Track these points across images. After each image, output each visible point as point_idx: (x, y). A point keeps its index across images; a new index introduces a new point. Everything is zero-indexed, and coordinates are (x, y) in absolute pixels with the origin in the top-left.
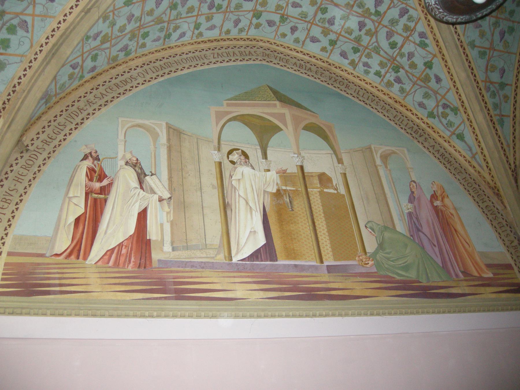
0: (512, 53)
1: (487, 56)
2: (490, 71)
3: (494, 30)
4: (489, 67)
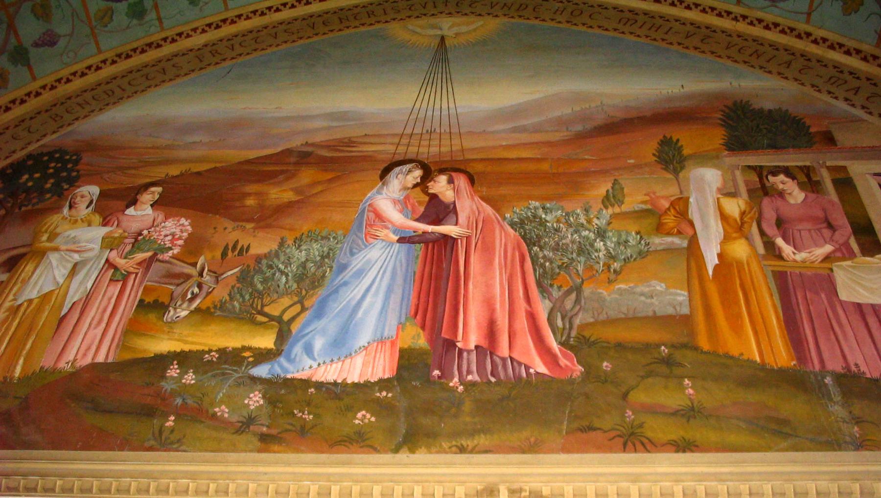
0: (97, 44)
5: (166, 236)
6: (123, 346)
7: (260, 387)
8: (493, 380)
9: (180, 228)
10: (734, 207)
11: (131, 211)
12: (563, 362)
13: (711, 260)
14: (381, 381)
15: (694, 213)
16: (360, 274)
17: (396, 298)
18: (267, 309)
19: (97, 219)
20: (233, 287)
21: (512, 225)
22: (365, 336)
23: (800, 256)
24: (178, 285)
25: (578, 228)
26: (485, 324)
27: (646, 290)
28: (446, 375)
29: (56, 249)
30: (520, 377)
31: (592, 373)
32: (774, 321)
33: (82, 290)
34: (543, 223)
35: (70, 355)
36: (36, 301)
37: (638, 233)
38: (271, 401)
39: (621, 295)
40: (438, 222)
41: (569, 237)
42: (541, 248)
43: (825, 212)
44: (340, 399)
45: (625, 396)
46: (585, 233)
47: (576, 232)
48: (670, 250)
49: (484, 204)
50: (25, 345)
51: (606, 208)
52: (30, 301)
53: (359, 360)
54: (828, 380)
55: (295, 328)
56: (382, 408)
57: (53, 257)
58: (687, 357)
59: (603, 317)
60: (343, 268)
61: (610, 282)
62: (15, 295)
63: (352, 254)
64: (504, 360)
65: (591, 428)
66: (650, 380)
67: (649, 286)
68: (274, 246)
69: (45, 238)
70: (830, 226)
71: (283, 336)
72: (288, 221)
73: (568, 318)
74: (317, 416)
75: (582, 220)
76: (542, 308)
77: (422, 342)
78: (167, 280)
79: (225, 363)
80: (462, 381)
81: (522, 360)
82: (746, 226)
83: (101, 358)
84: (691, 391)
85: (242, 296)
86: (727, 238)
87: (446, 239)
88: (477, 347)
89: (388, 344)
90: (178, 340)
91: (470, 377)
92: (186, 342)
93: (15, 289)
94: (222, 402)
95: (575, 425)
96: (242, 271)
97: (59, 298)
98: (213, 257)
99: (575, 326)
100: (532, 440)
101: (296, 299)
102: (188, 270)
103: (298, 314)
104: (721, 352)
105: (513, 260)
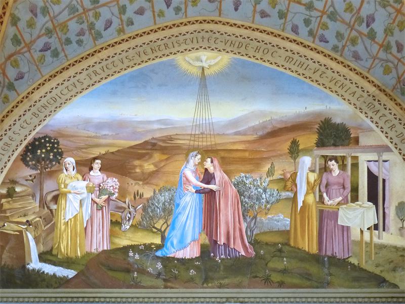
1: (18, 48)
2: (11, 63)
3: (43, 35)
4: (12, 59)
5: (110, 187)
6: (111, 242)
7: (160, 260)
8: (229, 258)
9: (114, 183)
10: (313, 177)
11: (91, 173)
12: (250, 250)
13: (300, 204)
14: (196, 257)
15: (298, 181)
16: (184, 208)
17: (197, 220)
18: (155, 226)
19: (80, 177)
20: (142, 214)
21: (235, 185)
22: (189, 239)
23: (331, 202)
24: (122, 212)
25: (257, 187)
26: (226, 234)
27: (277, 218)
28: (215, 256)
29: (70, 193)
30: (236, 257)
31: (257, 255)
32: (315, 233)
33: (88, 214)
34: (245, 184)
35: (94, 247)
36: (73, 219)
37: (277, 190)
38: (164, 266)
39: (269, 220)
40: (208, 183)
41: (254, 192)
42: (244, 197)
43: (344, 180)
44: (185, 265)
45: (266, 264)
46: (259, 190)
47: (256, 189)
48: (287, 199)
49: (225, 174)
50: (77, 242)
51: (268, 177)
52: (70, 219)
53: (188, 249)
54: (326, 259)
55: (166, 234)
56: (197, 268)
57: (70, 196)
58: (286, 248)
59: (262, 231)
60: (178, 205)
61: (266, 214)
62: (63, 216)
63: (180, 199)
64: (232, 249)
65: (256, 277)
66: (274, 258)
67: (278, 216)
68: (152, 194)
69: (63, 186)
70: (344, 188)
71: (163, 238)
72: (154, 181)
73: (252, 231)
74: (179, 272)
75: (259, 184)
76: (244, 226)
77: (207, 242)
78: (116, 210)
79: (147, 250)
80: (220, 258)
81: (237, 250)
82: (315, 187)
83: (105, 248)
84: (286, 263)
85: (146, 219)
86: (307, 194)
87: (212, 192)
88: (224, 243)
89: (197, 242)
90: (129, 240)
91: (222, 256)
92: (132, 241)
93: (62, 213)
94: (150, 267)
95: (252, 276)
96: (143, 206)
97: (81, 218)
98: (131, 199)
99: (254, 235)
100: (240, 281)
101: (164, 221)
102: (124, 205)
103: (166, 228)
104: (297, 247)
105: (235, 202)
